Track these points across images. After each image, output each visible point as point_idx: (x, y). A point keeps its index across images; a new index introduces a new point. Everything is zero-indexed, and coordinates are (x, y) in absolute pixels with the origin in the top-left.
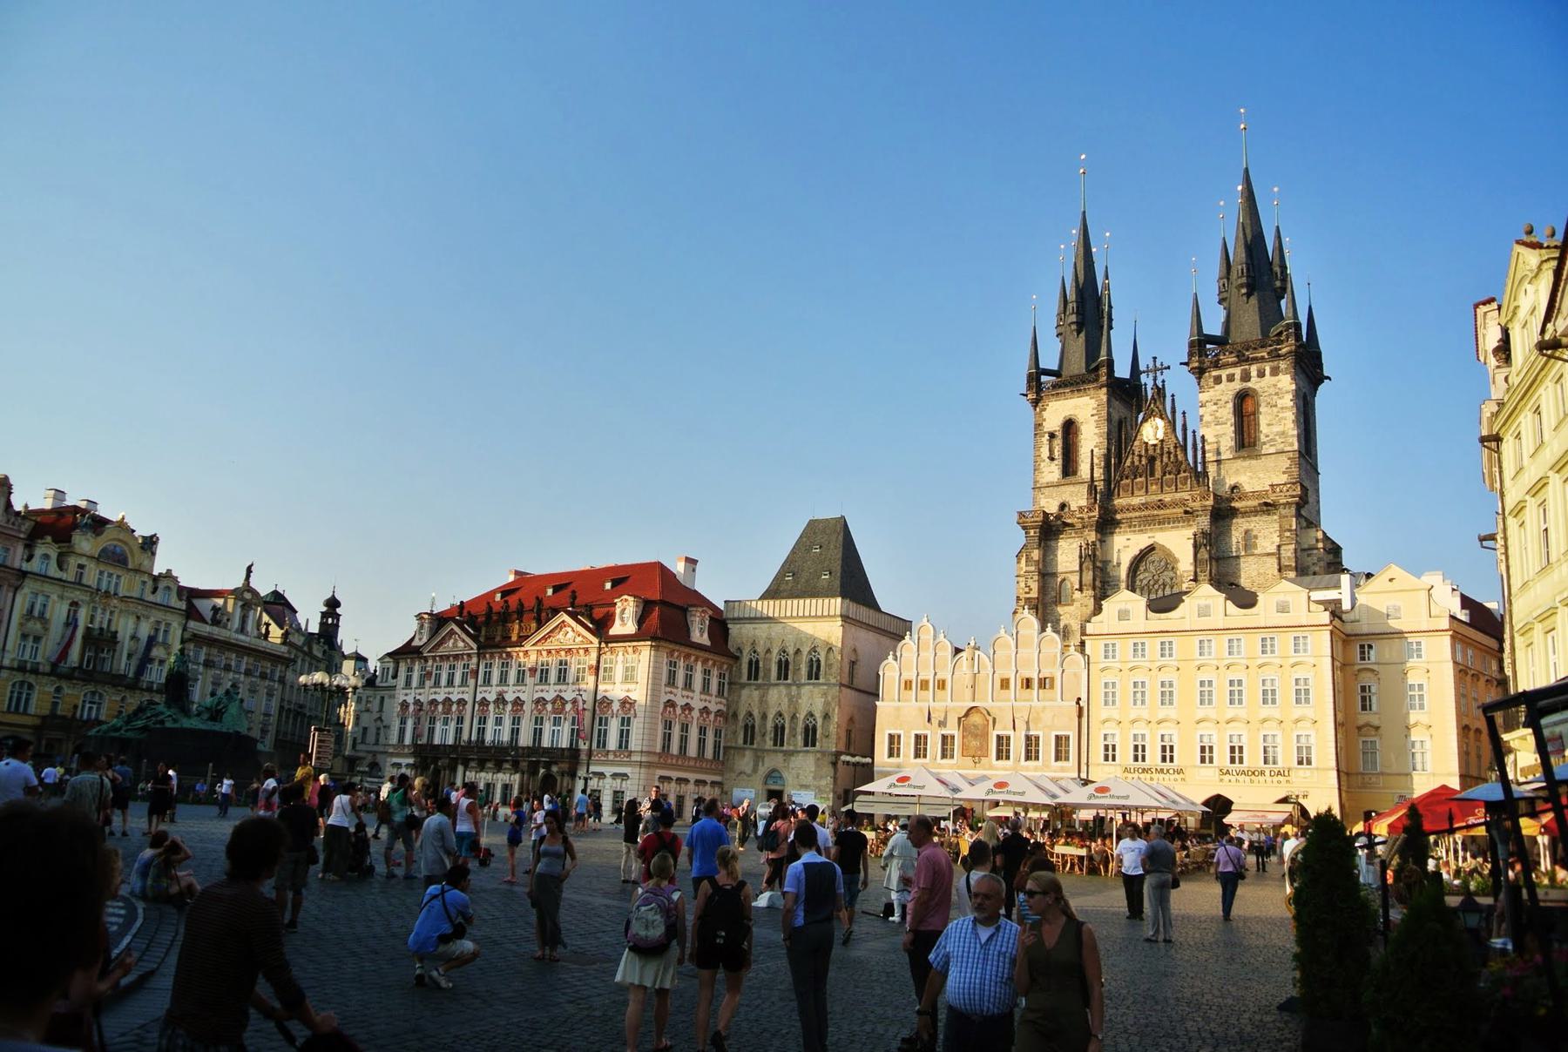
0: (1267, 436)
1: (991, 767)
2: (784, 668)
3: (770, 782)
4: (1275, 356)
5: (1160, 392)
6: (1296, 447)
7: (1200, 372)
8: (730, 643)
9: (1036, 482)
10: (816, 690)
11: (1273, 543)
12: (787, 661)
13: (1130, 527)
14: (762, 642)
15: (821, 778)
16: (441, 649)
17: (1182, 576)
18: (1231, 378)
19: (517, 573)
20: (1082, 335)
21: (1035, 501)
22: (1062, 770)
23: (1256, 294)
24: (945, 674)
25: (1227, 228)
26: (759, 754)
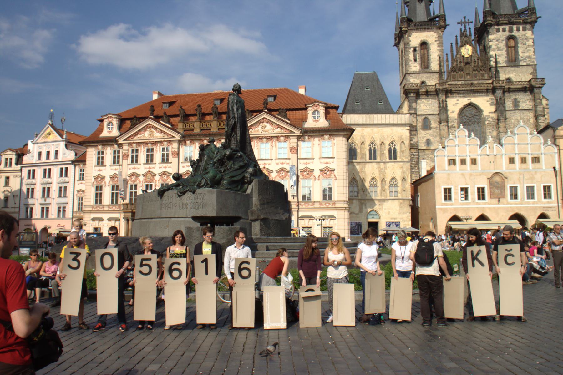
0: (522, 57)
1: (508, 203)
2: (373, 153)
4: (525, 23)
10: (396, 165)
11: (527, 105)
12: (375, 149)
13: (458, 94)
14: (358, 138)
15: (404, 213)
16: (136, 138)
17: (485, 118)
18: (504, 30)
19: (160, 94)
22: (548, 203)
26: (362, 202)
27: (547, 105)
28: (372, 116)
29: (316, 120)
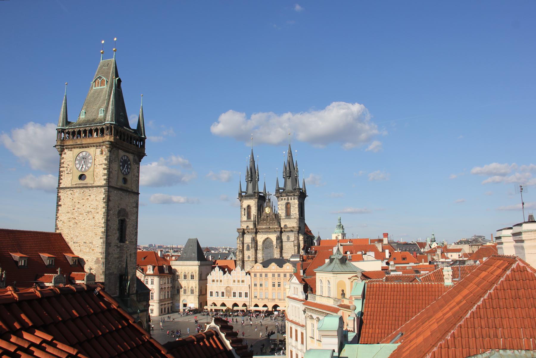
1: (232, 299)
2: (185, 277)
3: (184, 301)
5: (269, 200)
6: (298, 217)
7: (278, 197)
8: (172, 271)
9: (241, 220)
14: (180, 270)
18: (285, 199)
20: (252, 183)
21: (241, 225)
22: (246, 299)
23: (290, 178)
24: (222, 279)
25: (285, 159)
27: (302, 239)
28: (184, 262)
29: (150, 271)
